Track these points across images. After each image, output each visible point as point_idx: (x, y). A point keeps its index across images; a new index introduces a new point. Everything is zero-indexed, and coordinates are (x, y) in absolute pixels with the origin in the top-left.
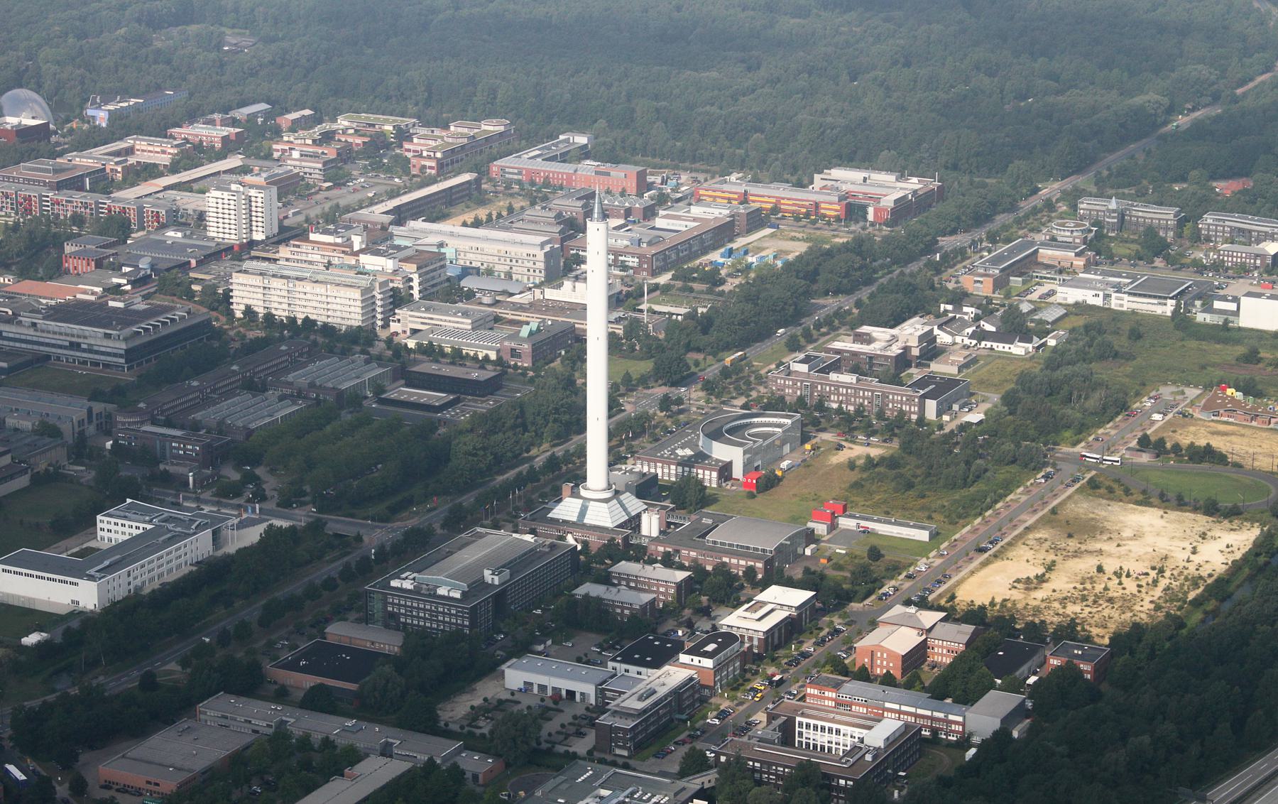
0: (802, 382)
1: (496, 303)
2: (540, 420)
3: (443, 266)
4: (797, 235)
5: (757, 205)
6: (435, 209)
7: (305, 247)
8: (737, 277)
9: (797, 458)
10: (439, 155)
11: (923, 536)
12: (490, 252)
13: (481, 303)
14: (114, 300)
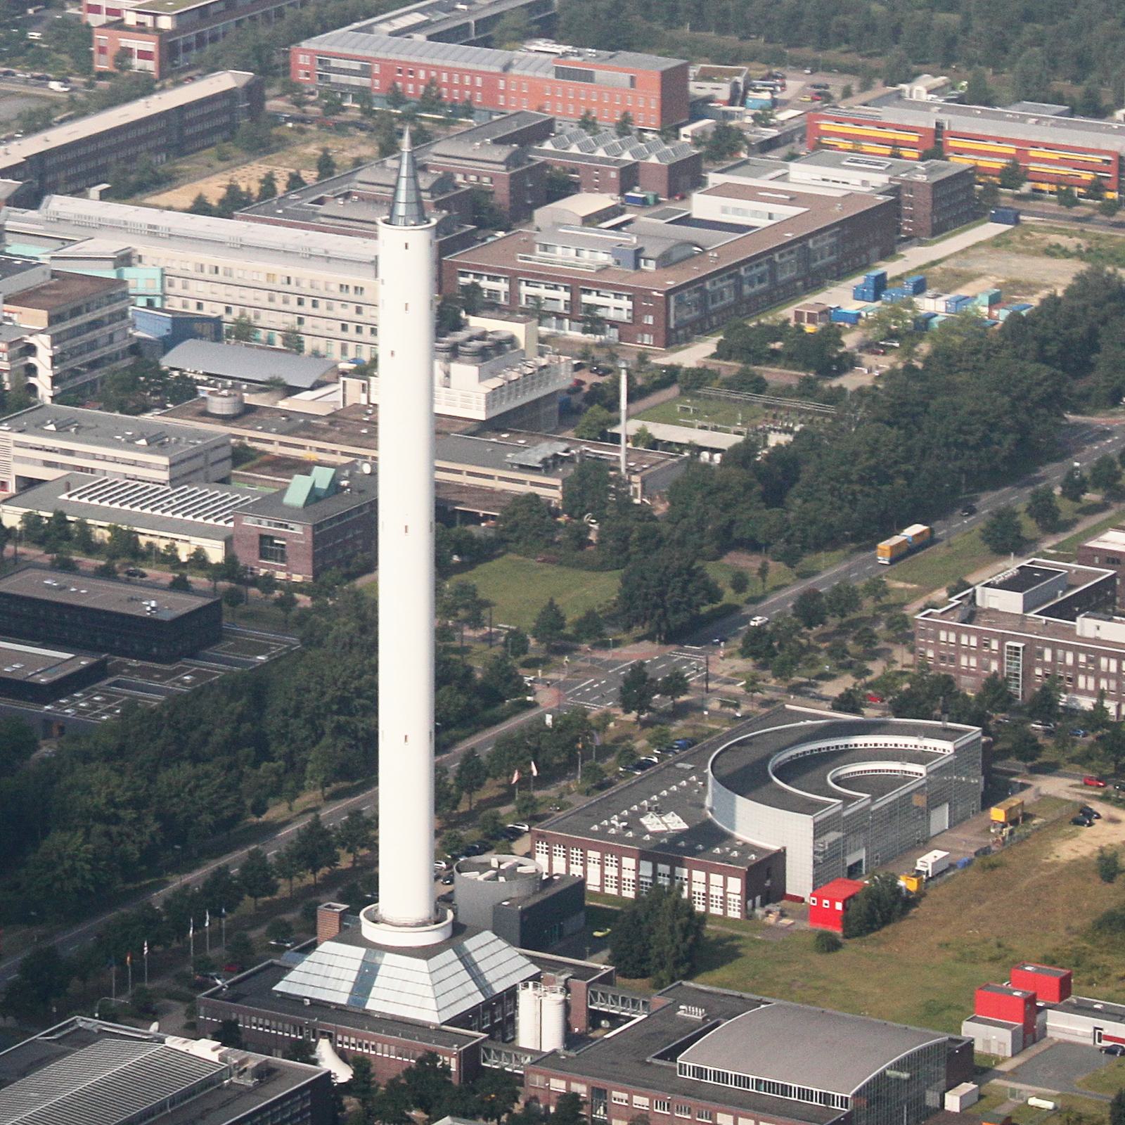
0: (1003, 638)
1: (245, 413)
2: (299, 729)
3: (123, 314)
4: (1064, 241)
5: (964, 162)
6: (127, 167)
8: (886, 351)
9: (967, 842)
10: (166, 23)
12: (249, 279)
13: (205, 414)
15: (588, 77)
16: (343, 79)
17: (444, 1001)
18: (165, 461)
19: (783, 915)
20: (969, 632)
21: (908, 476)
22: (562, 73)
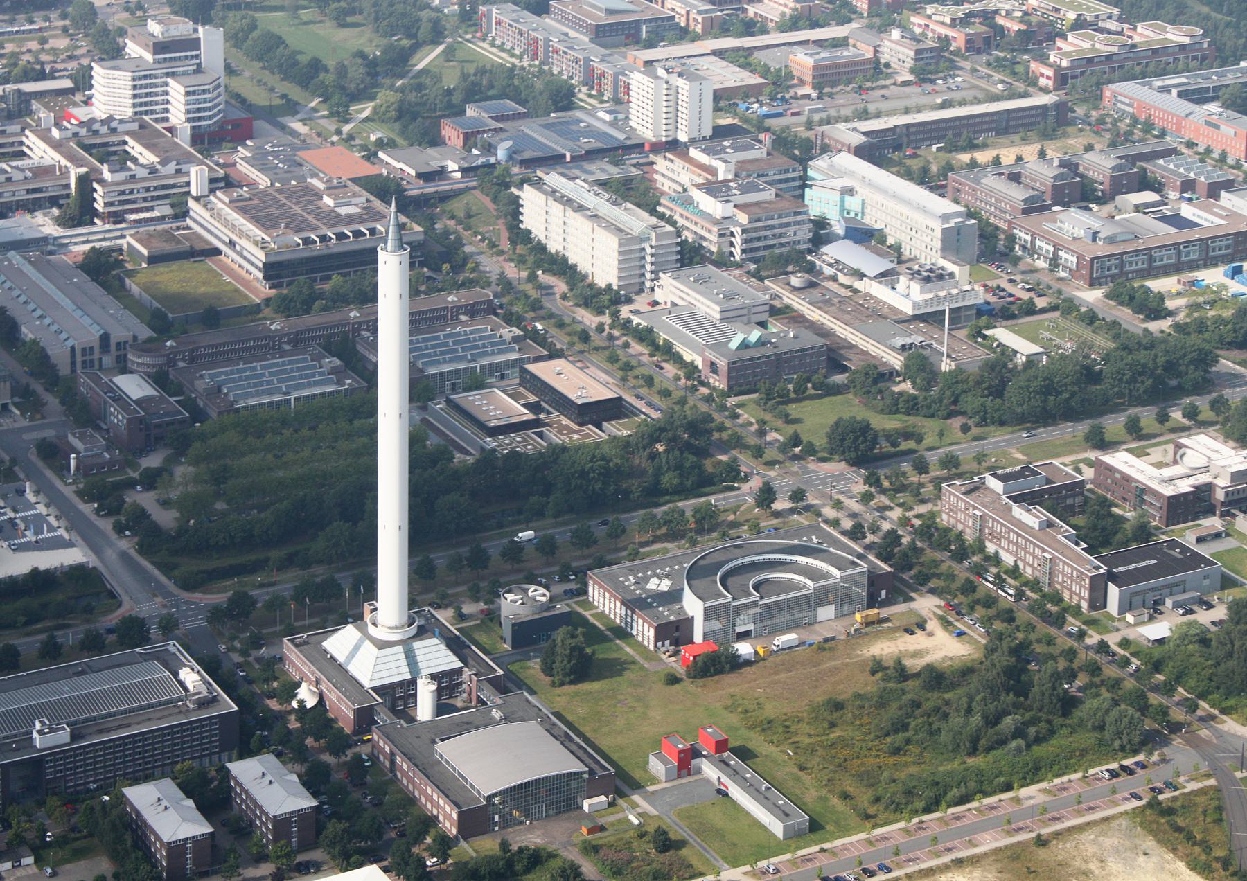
7: (679, 163)
10: (1065, 64)
11: (777, 827)
14: (329, 196)
15: (1217, 127)
16: (1122, 106)
17: (377, 675)
18: (718, 309)
19: (676, 653)
20: (963, 500)
21: (1073, 395)
22: (1208, 123)
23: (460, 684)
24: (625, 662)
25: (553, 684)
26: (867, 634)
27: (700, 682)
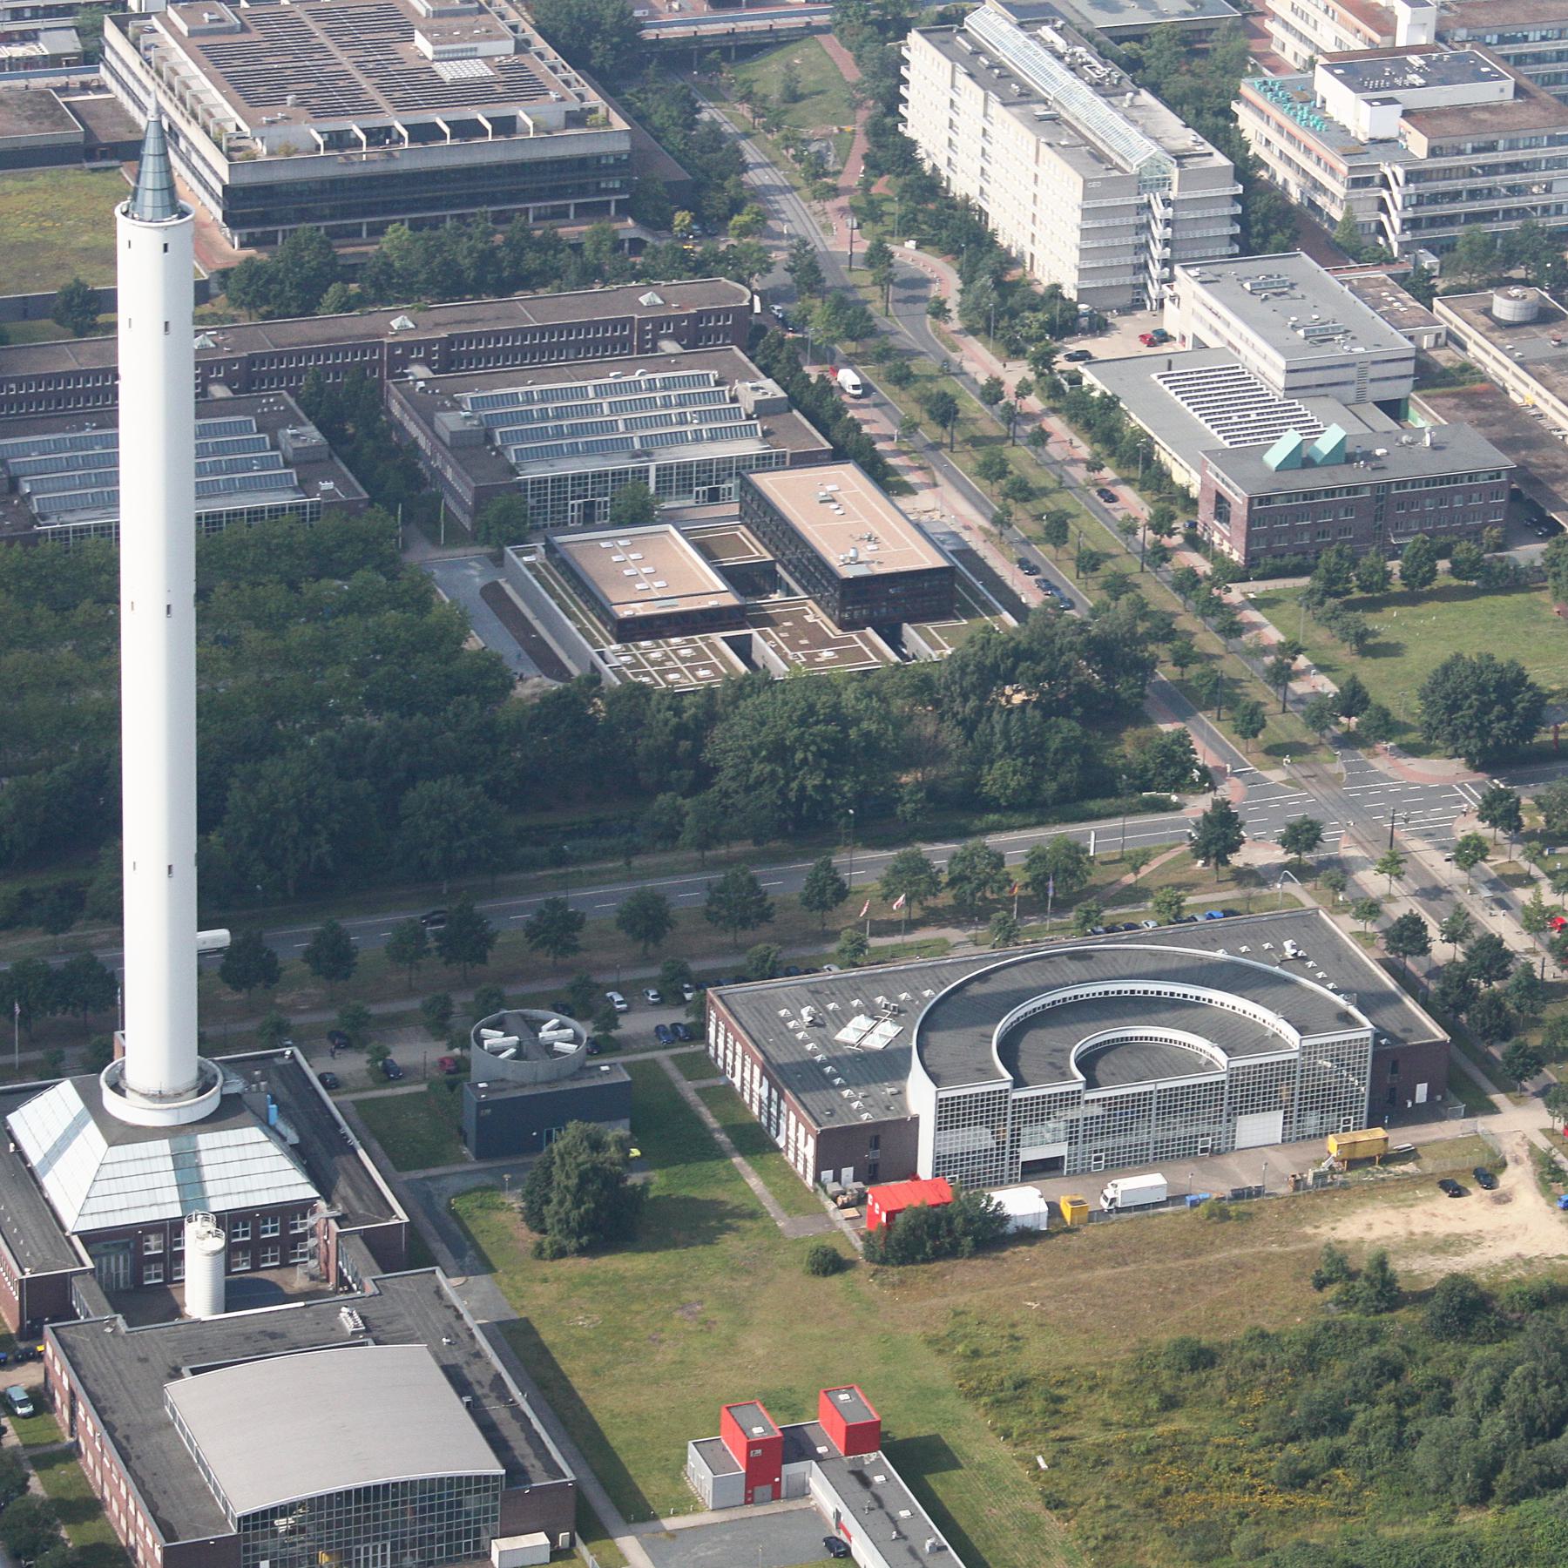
23: (303, 1237)
24: (738, 1213)
25: (539, 1252)
26: (1345, 1186)
27: (894, 1274)
